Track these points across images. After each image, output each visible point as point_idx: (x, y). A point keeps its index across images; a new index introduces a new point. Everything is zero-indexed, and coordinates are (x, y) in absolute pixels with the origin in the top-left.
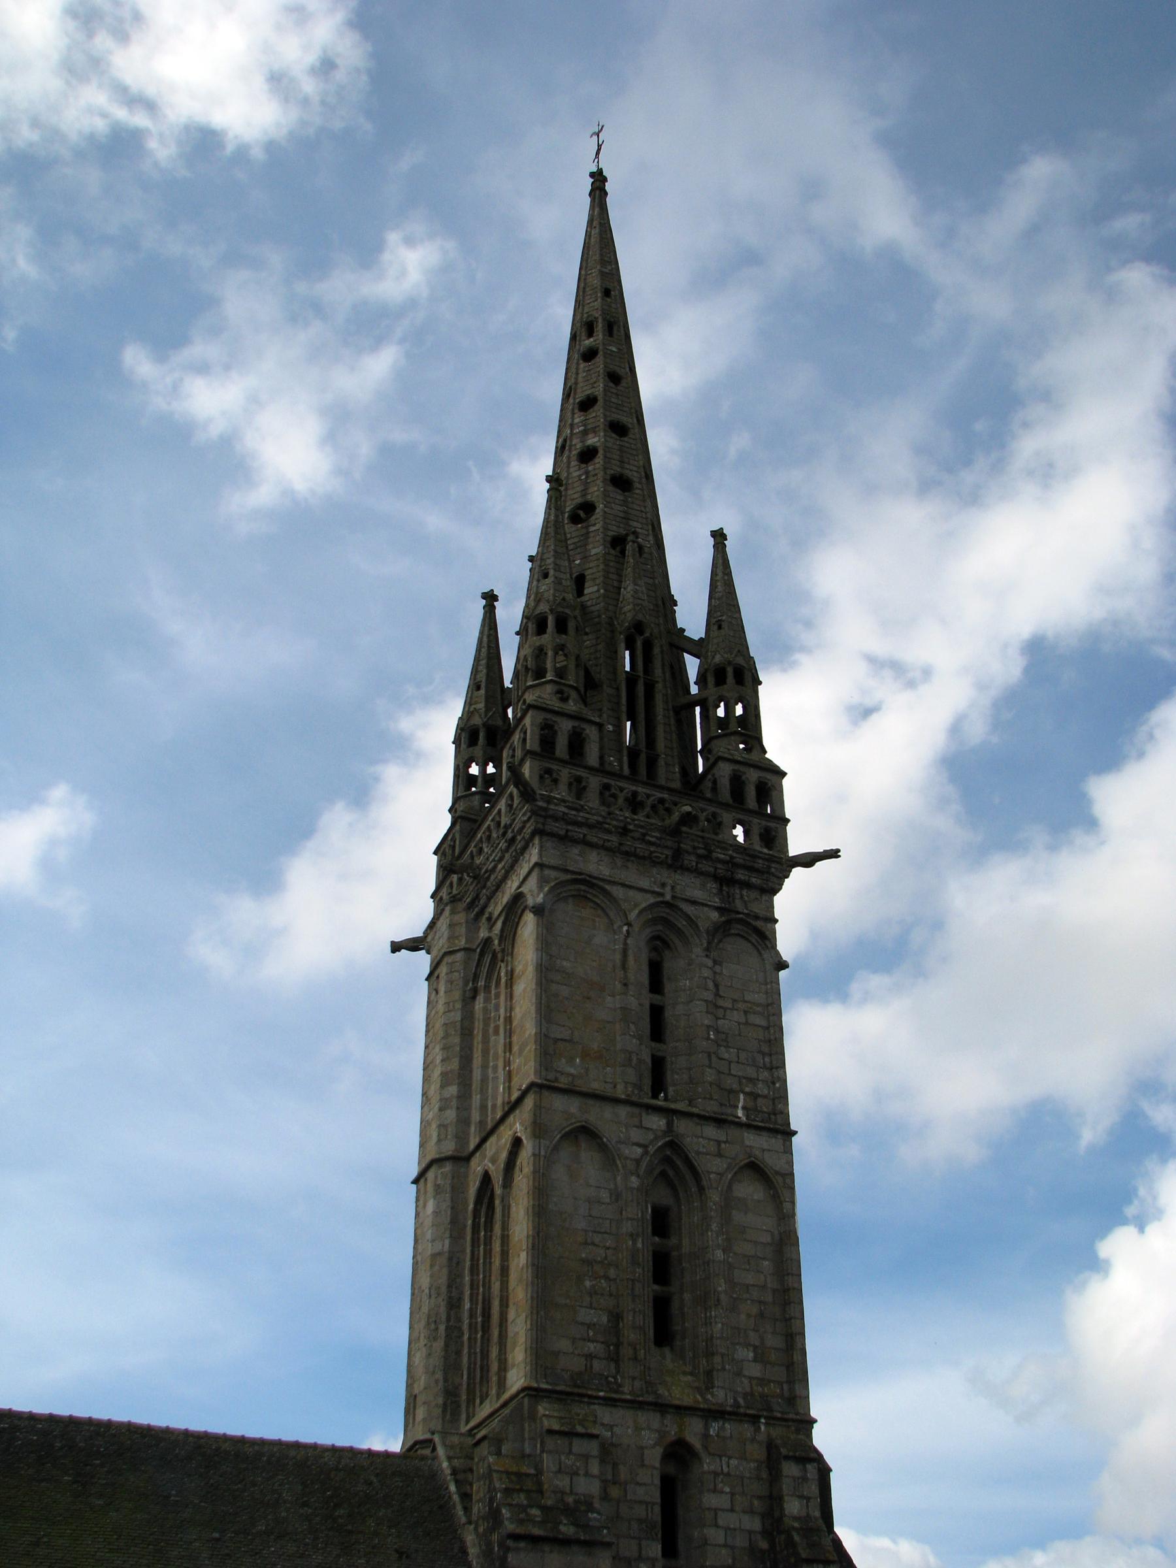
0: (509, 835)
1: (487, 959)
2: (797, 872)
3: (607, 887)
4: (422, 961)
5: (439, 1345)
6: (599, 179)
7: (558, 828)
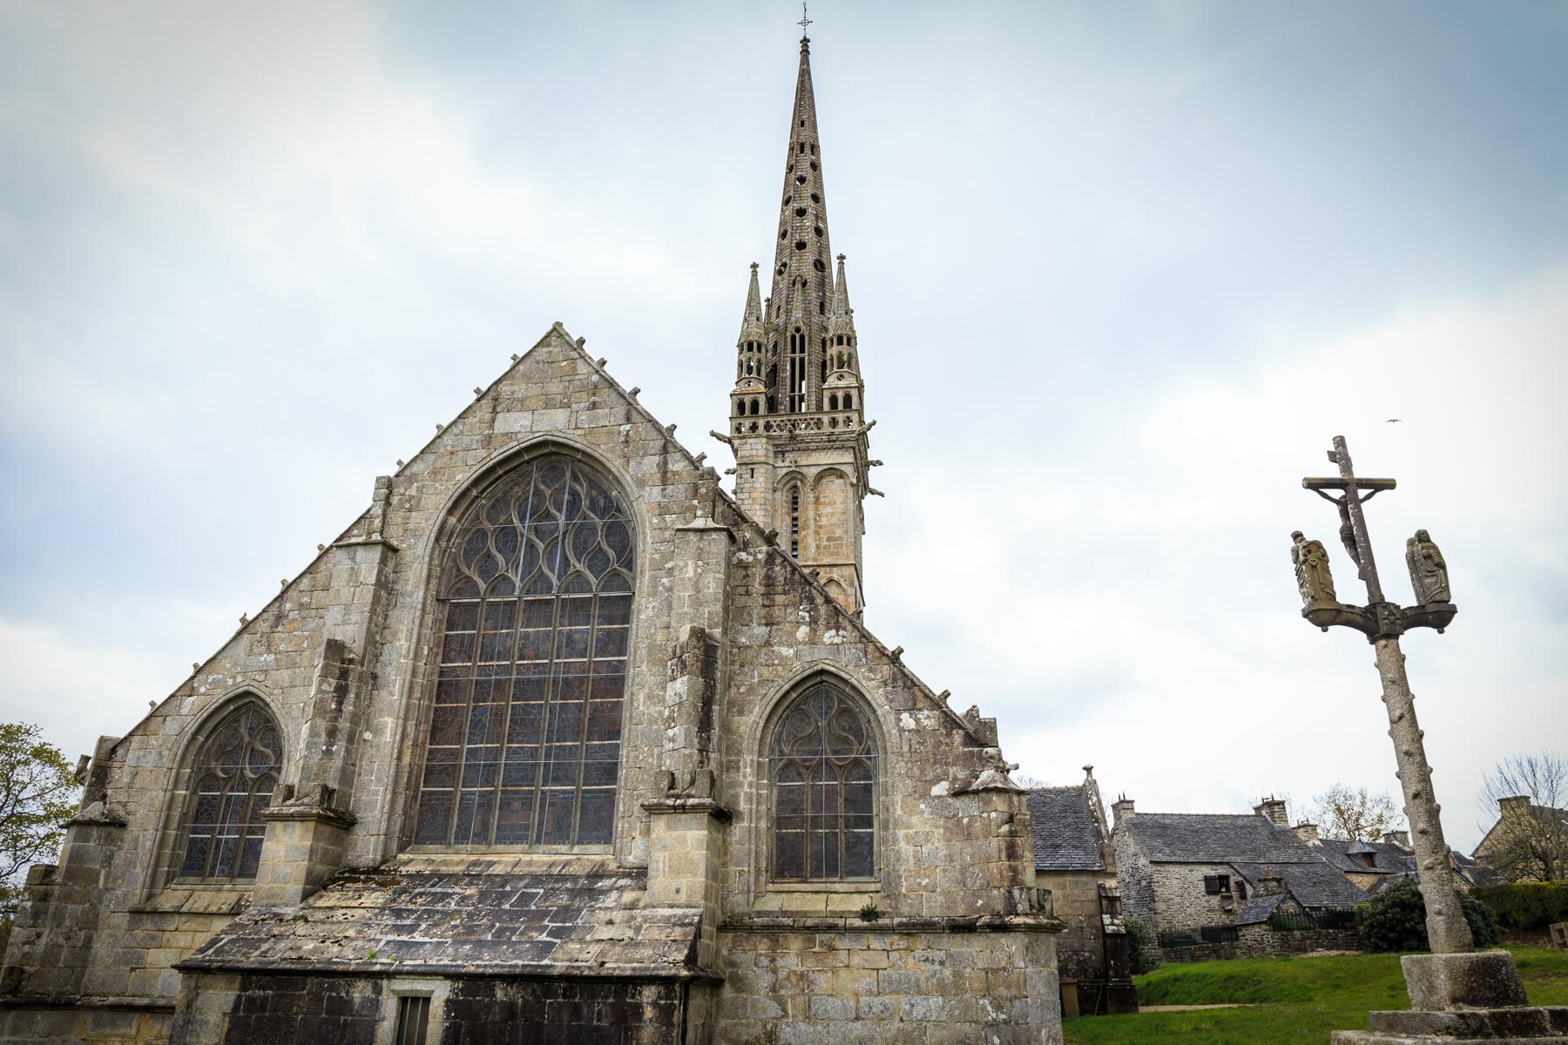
0: (834, 438)
6: (805, 41)
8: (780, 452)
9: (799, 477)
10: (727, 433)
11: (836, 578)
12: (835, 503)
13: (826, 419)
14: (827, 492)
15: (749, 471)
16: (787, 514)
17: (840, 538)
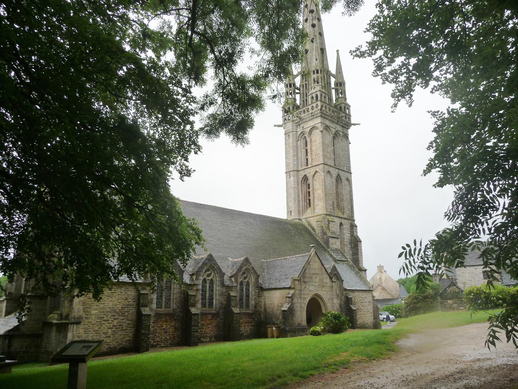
1: (301, 135)
2: (352, 126)
3: (330, 128)
4: (282, 131)
5: (296, 203)
7: (323, 115)
8: (298, 125)
10: (281, 123)
13: (310, 107)
15: (288, 136)
16: (303, 148)
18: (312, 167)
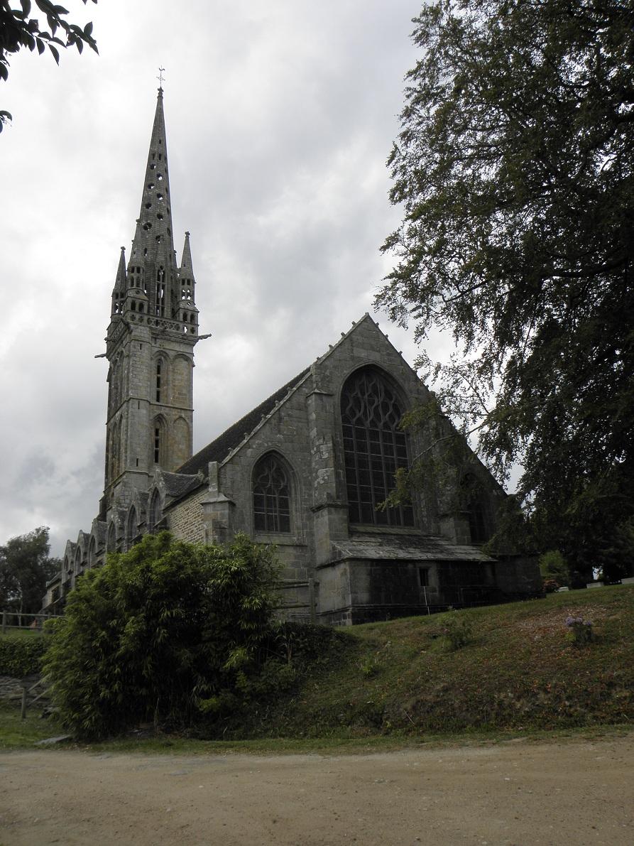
0: (185, 337)
9: (164, 354)
11: (183, 416)
12: (183, 374)
14: (179, 367)
17: (185, 395)
18: (174, 408)
